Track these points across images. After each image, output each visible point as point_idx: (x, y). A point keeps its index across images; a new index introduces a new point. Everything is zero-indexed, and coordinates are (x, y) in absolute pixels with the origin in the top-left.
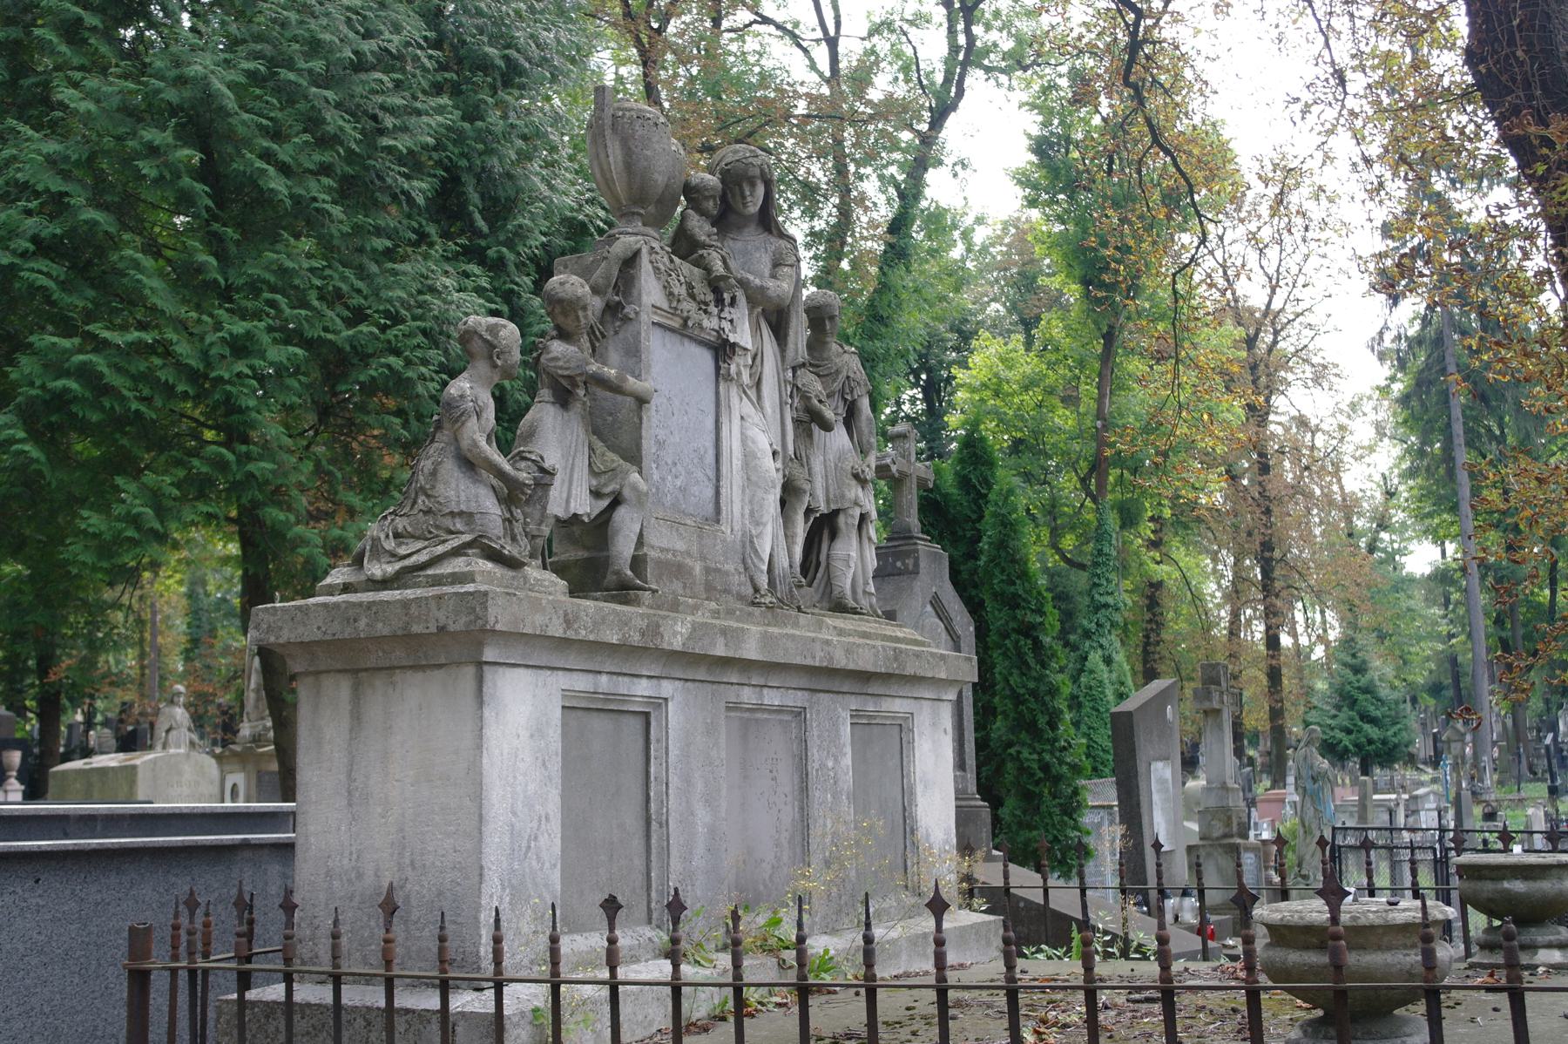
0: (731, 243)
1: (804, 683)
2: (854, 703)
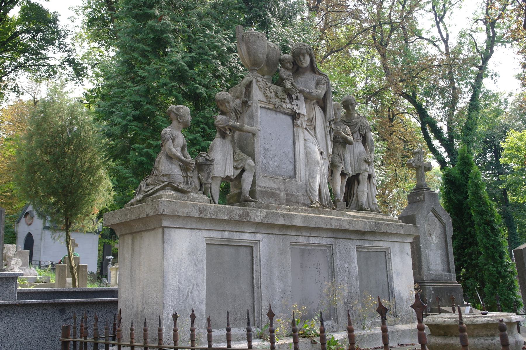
0: (300, 78)
1: (330, 235)
2: (358, 243)
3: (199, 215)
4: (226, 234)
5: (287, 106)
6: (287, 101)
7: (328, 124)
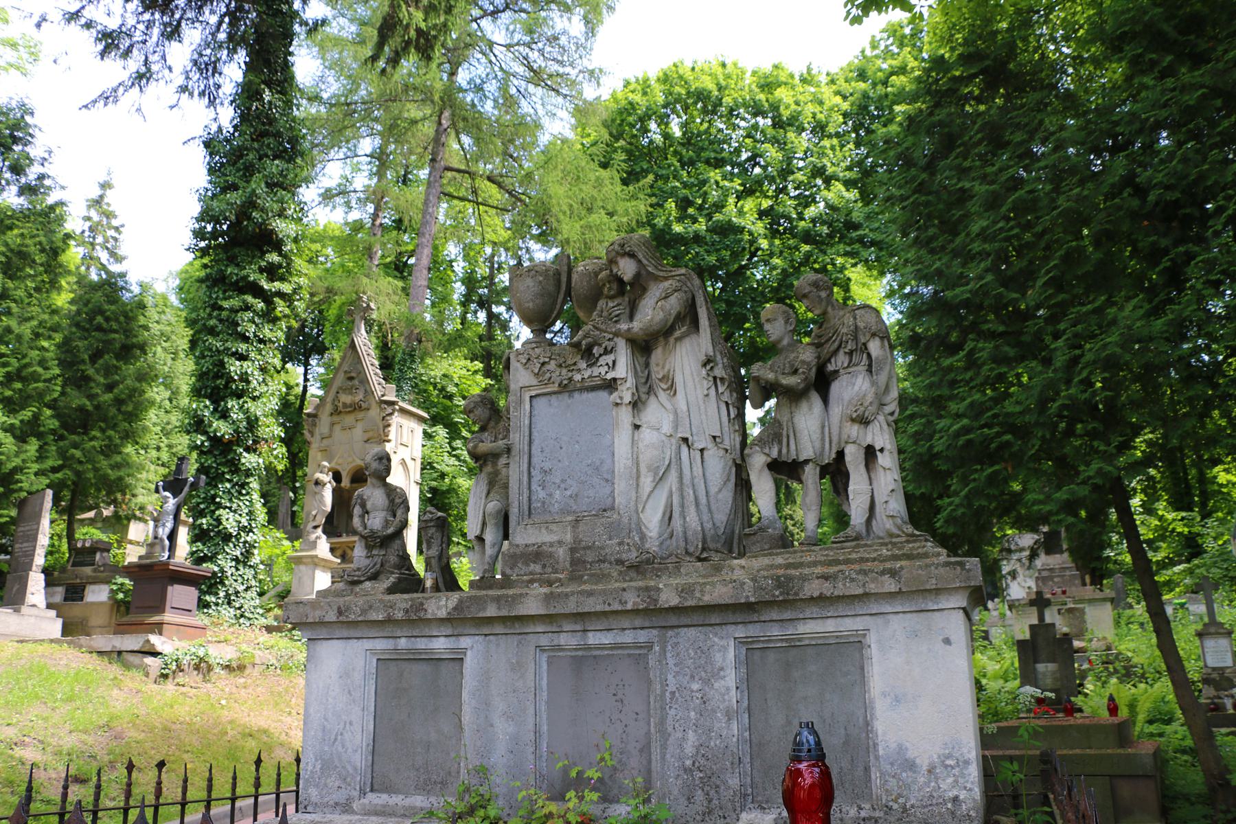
1: (638, 623)
2: (740, 632)
4: (403, 643)
5: (585, 372)
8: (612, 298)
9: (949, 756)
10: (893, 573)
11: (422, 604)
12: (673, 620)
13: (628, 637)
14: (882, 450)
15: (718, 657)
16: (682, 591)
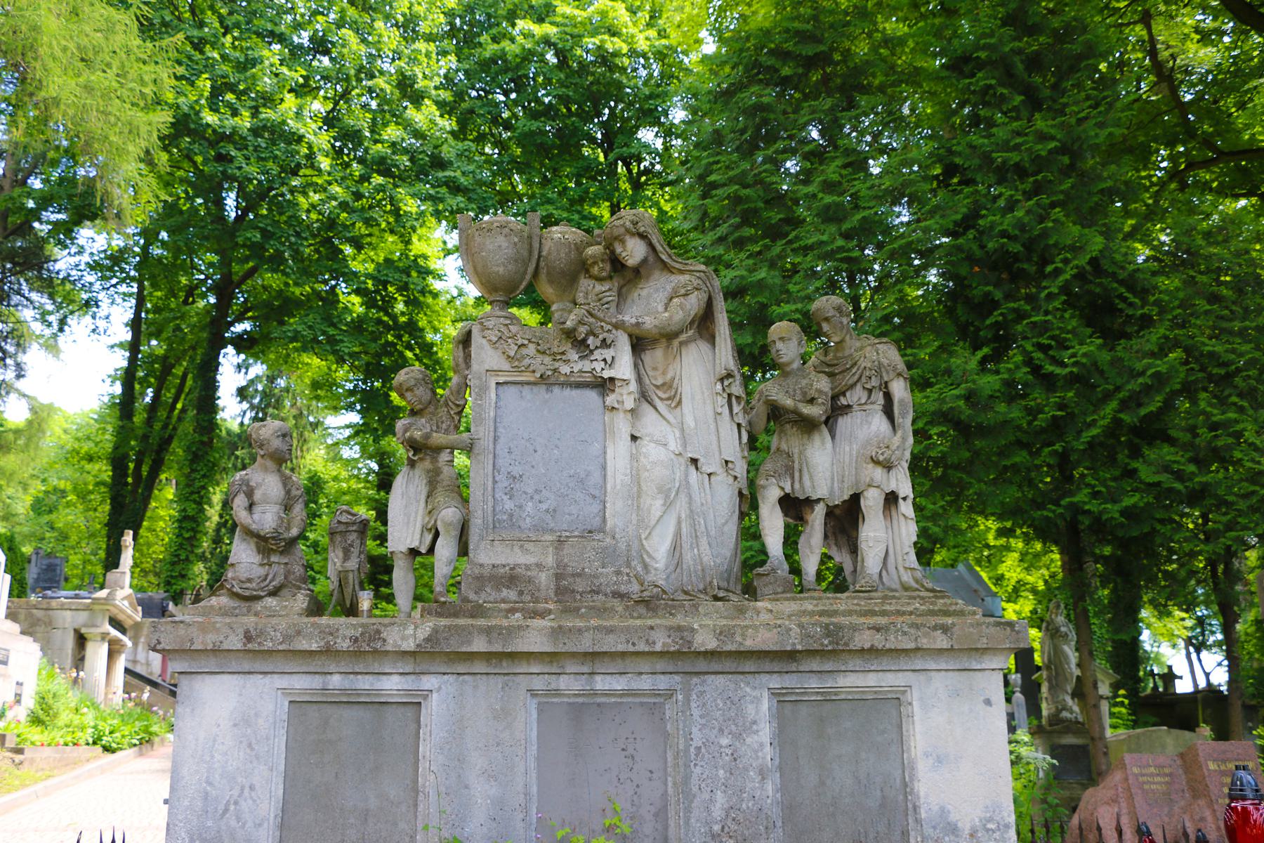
2: (775, 682)
3: (245, 645)
4: (336, 681)
5: (575, 365)
6: (573, 355)
7: (719, 386)
8: (600, 279)
9: (990, 820)
10: (945, 629)
11: (378, 632)
12: (702, 665)
13: (645, 683)
14: (904, 499)
15: (750, 709)
16: (721, 633)
